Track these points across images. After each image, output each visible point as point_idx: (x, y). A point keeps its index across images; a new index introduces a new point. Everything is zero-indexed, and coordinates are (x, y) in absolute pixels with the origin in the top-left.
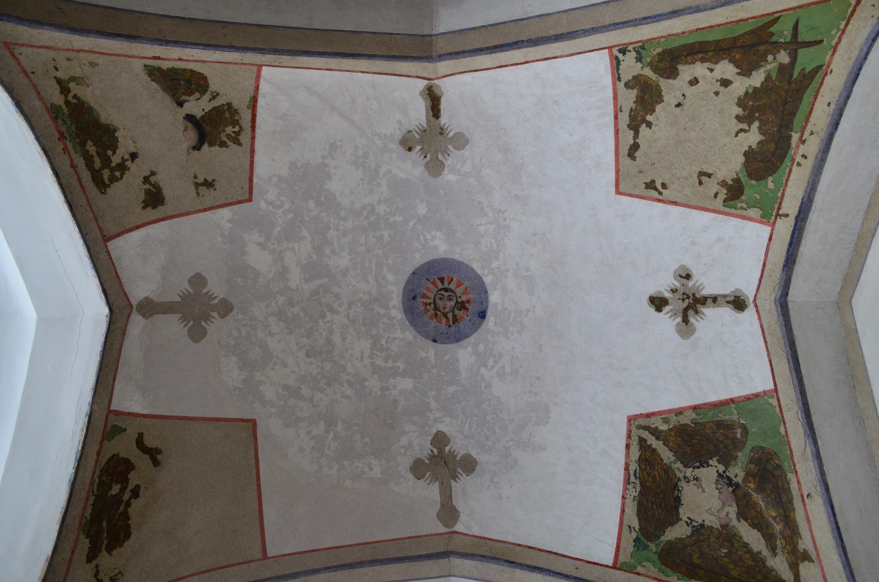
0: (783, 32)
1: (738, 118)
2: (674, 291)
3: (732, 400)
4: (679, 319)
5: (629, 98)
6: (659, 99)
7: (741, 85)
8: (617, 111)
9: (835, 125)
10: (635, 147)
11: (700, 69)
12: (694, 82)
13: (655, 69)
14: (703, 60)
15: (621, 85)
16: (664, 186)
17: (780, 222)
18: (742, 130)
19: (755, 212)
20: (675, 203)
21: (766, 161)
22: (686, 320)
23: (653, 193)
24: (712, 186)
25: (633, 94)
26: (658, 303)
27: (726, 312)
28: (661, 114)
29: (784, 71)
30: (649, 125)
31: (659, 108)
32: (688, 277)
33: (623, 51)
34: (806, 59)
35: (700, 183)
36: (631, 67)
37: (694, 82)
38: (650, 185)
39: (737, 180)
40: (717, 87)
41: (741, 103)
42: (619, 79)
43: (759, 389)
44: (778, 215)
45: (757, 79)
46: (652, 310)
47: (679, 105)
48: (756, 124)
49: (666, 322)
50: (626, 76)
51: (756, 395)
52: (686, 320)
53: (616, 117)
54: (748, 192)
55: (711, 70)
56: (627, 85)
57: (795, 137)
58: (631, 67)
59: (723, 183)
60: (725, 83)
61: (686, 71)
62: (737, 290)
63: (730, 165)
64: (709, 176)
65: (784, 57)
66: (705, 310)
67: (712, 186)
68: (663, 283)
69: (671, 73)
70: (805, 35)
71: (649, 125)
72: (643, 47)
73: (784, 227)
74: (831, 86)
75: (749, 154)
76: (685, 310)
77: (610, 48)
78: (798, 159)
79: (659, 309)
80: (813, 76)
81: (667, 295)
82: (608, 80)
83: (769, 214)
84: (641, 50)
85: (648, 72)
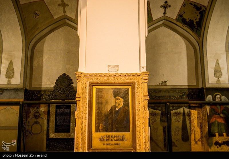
0: (199, 29)
1: (191, 19)
2: (168, 4)
3: (152, 15)
4: (163, 5)
5: (199, 6)
6: (197, 10)
7: (195, 21)
8: (198, 4)
9: (187, 31)
10: (191, 4)
11: (199, 17)
12: (197, 16)
13: (201, 11)
14: (200, 18)
15: (201, 6)
16: (184, 7)
17: (175, 21)
18: (189, 19)
19: (177, 18)
20: (181, 7)
21: (184, 21)
22: (163, 6)
23: (184, 5)
24: (182, 13)
25: (199, 7)
26: (166, 2)
27: (163, 12)
28: (195, 9)
29: (195, 27)
30: (194, 7)
31: (196, 10)
32: (169, 7)
33: (206, 9)
34: (195, 30)
35: (183, 12)
36: (203, 8)
37: (197, 16)
38: (185, 5)
39: (182, 17)
40: (196, 18)
41: (193, 20)
42: (202, 6)
43: (153, 18)
44: (176, 21)
45: (195, 23)
46: (165, 1)
47: (195, 12)
48: (189, 21)
49: (162, 3)
50: (202, 7)
51: (152, 18)
52: (163, 6)
53: (197, 3)
54: (181, 18)
55: (198, 18)
56: (201, 7)
57: (186, 26)
58: (203, 8)
59: (182, 15)
60: (196, 19)
61: (199, 15)
62: (166, 13)
63: (185, 16)
64: (184, 13)
65: (196, 27)
66: (164, 9)
67: (182, 13)
68: (169, 3)
69: (200, 13)
70: (198, 30)
71: (194, 7)
72: (205, 12)
73: (174, 22)
74: (191, 32)
75: (185, 19)
76: (164, 6)
77: (207, 7)
78: (183, 26)
79: (165, 2)
80: (192, 30)
81: (167, 4)
82: (203, 4)
83: (177, 20)
84: (205, 11)
85: (201, 10)
